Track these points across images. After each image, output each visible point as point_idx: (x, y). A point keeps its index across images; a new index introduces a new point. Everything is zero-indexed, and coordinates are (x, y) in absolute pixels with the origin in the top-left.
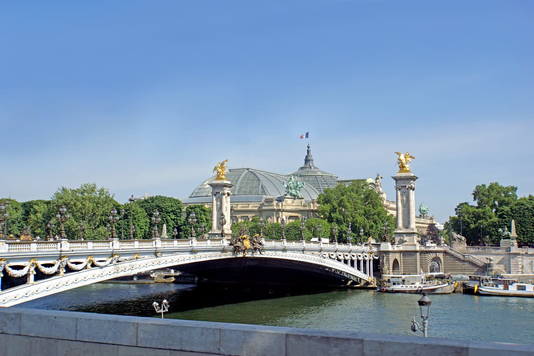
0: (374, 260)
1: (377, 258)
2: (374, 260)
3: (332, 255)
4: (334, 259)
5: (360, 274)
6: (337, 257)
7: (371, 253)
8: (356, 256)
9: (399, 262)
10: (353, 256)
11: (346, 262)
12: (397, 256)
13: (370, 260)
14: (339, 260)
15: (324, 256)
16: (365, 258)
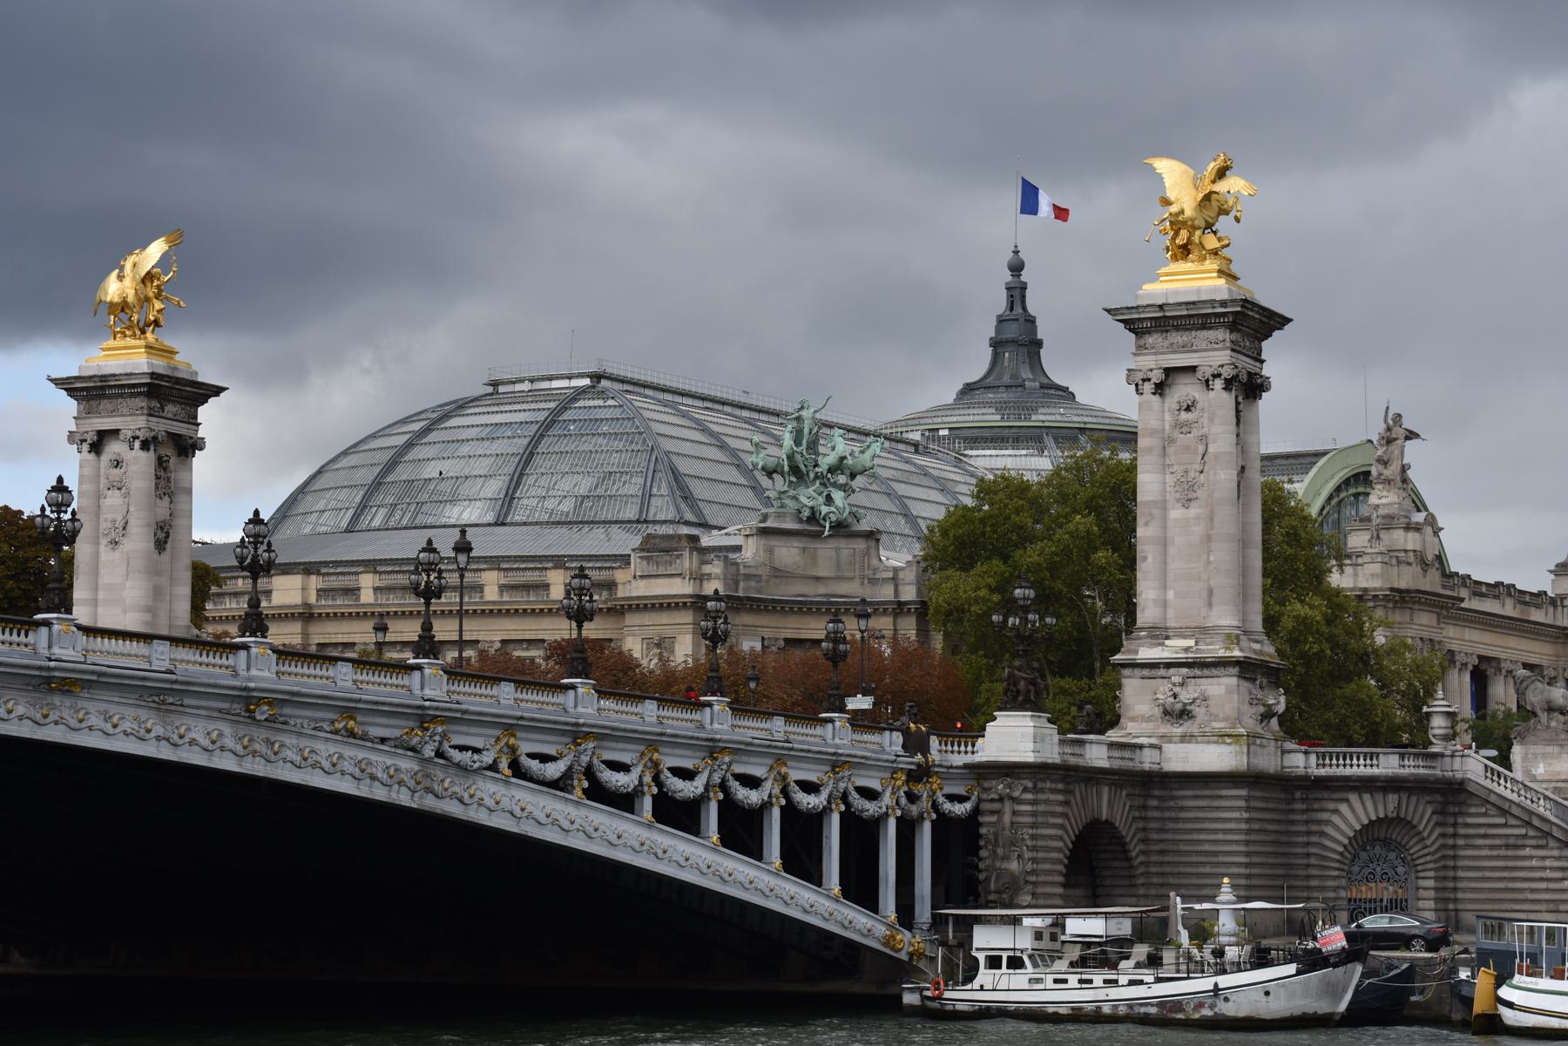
0: (943, 824)
1: (960, 809)
2: (943, 824)
3: (545, 758)
4: (560, 785)
5: (819, 905)
6: (589, 772)
7: (920, 774)
8: (770, 787)
9: (1135, 849)
10: (752, 782)
11: (678, 815)
12: (1106, 804)
13: (907, 829)
14: (598, 793)
15: (457, 756)
16: (858, 802)
